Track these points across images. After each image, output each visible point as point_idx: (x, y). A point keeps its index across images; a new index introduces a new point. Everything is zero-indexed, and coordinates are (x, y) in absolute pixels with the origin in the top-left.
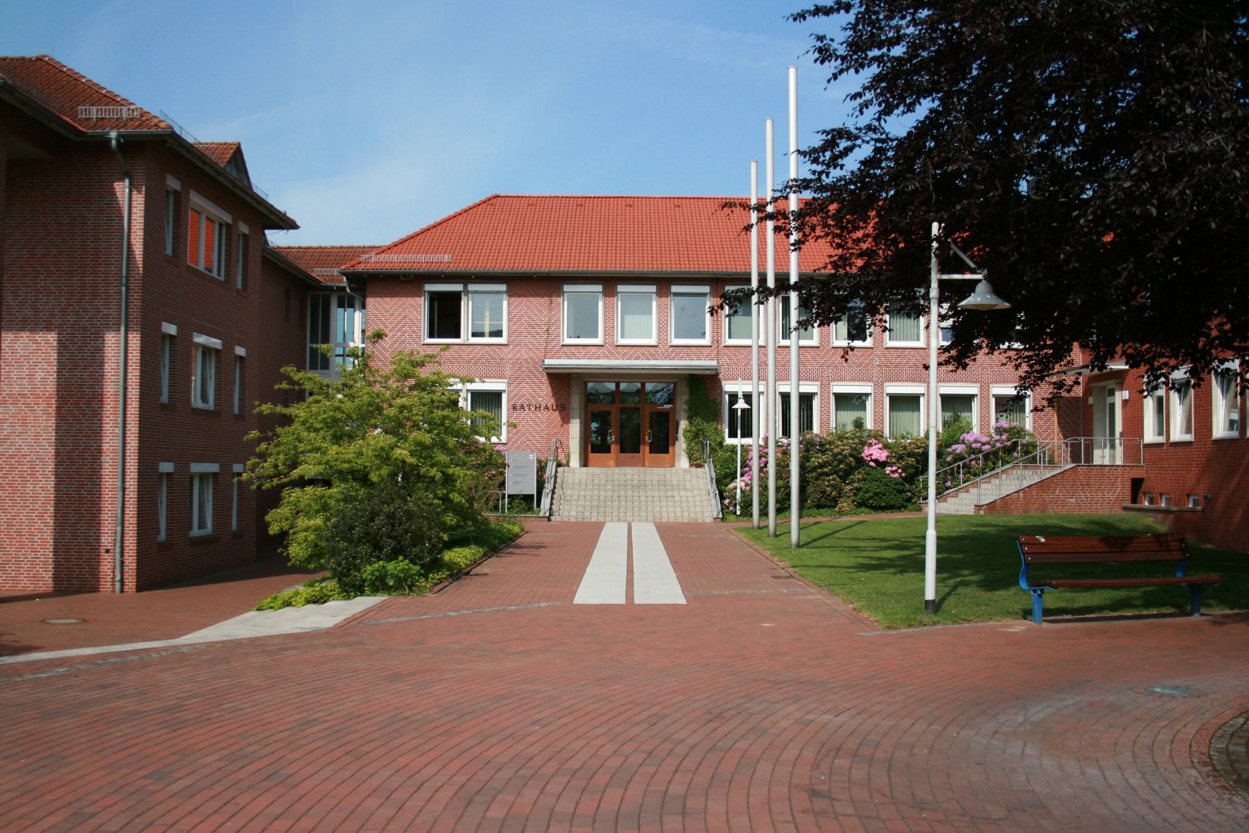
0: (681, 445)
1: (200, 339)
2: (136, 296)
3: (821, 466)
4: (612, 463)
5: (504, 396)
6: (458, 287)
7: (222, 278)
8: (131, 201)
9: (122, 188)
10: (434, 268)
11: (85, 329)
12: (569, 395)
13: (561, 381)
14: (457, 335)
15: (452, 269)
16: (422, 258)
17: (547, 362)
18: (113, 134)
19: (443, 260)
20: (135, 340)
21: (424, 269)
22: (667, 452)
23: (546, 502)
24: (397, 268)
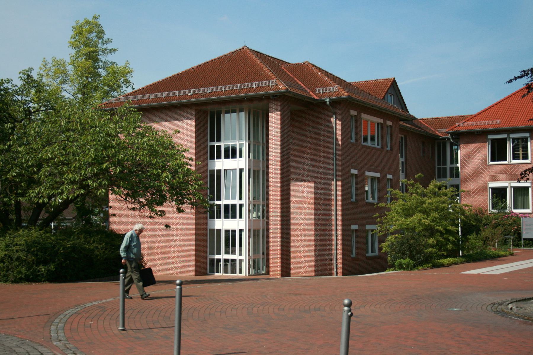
1: (368, 173)
2: (339, 160)
5: (530, 189)
6: (505, 136)
7: (379, 147)
9: (333, 119)
10: (491, 128)
11: (321, 174)
15: (500, 127)
16: (486, 122)
18: (328, 100)
19: (496, 123)
21: (486, 128)
24: (473, 129)
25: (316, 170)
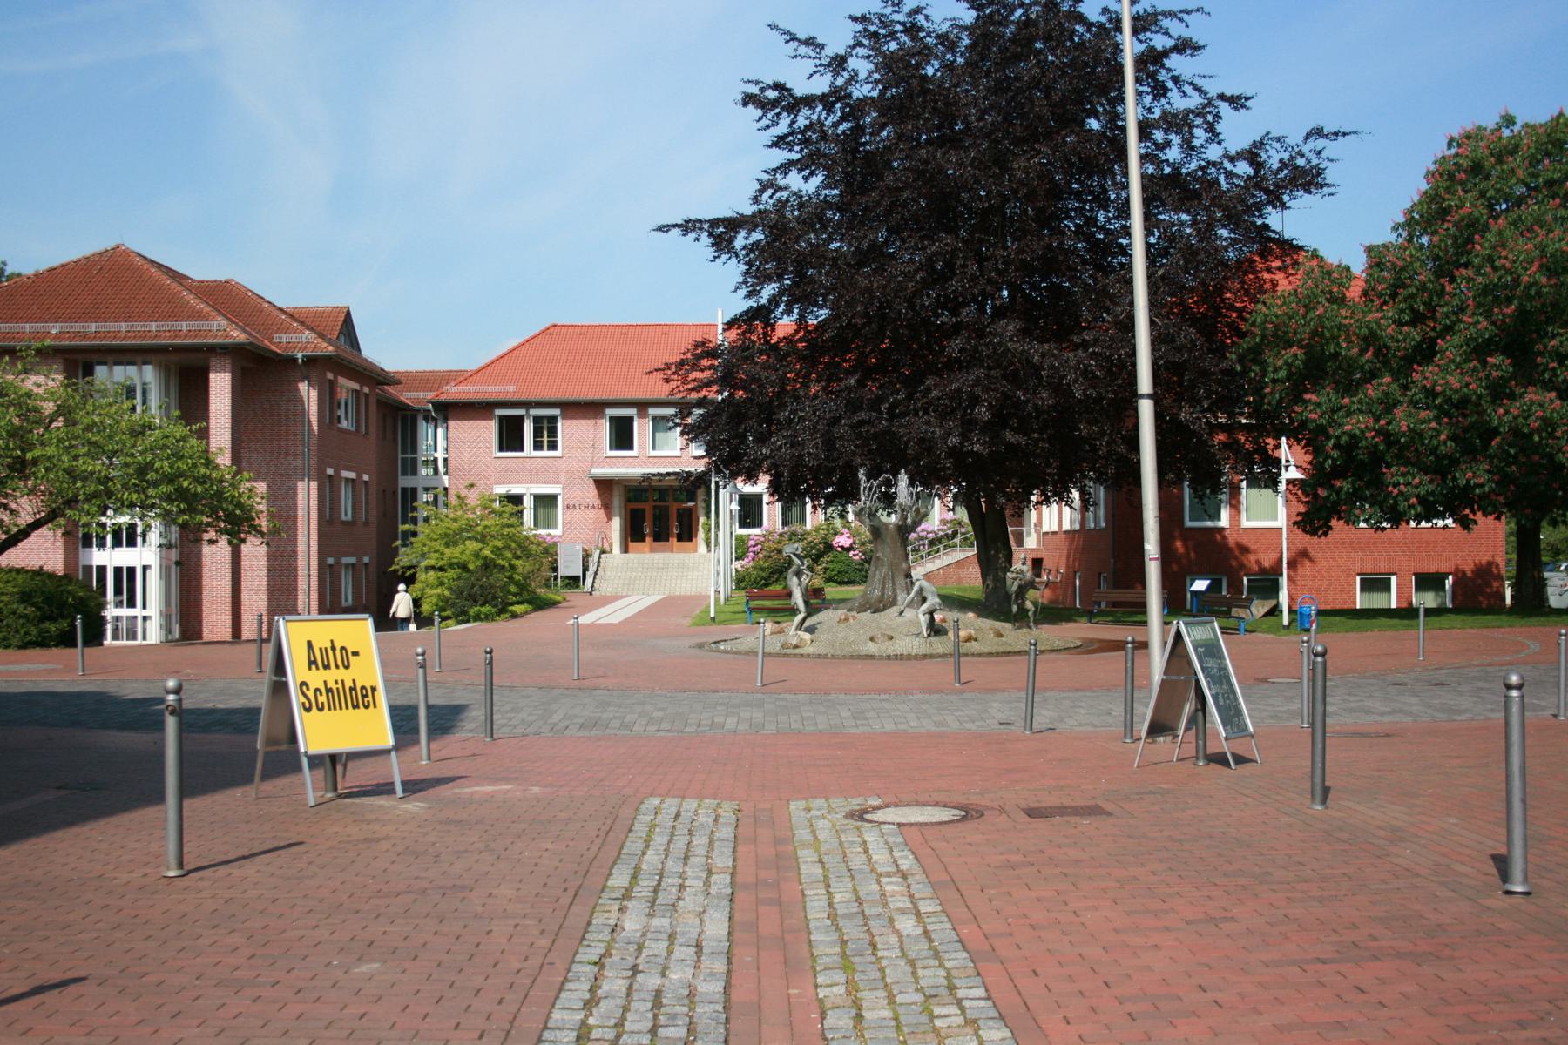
0: (701, 534)
2: (313, 454)
6: (521, 412)
8: (309, 395)
9: (303, 387)
10: (502, 397)
13: (604, 485)
14: (521, 449)
15: (516, 398)
16: (492, 388)
18: (299, 356)
19: (509, 391)
20: (314, 485)
21: (493, 398)
22: (690, 540)
23: (589, 581)
24: (472, 397)
25: (273, 469)
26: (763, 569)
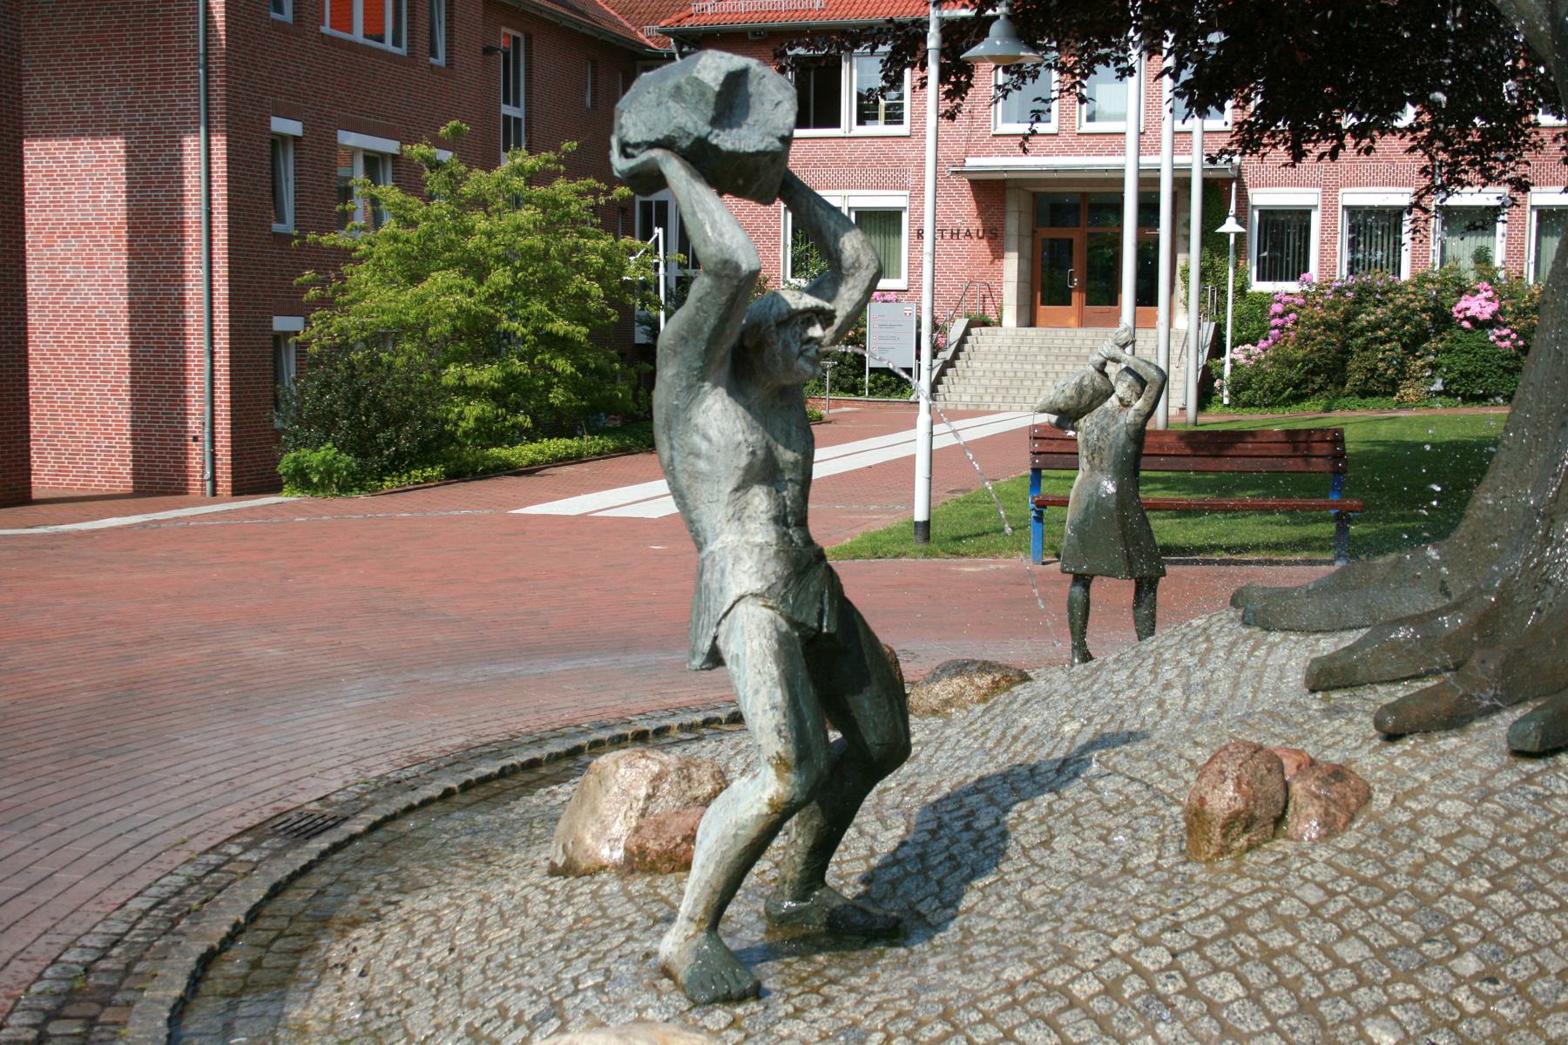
1: (349, 139)
2: (218, 81)
3: (1376, 326)
4: (1073, 321)
5: (905, 217)
7: (402, 51)
11: (157, 131)
12: (1003, 213)
13: (991, 191)
14: (835, 122)
17: (972, 162)
20: (219, 144)
25: (140, 117)
26: (1291, 364)
